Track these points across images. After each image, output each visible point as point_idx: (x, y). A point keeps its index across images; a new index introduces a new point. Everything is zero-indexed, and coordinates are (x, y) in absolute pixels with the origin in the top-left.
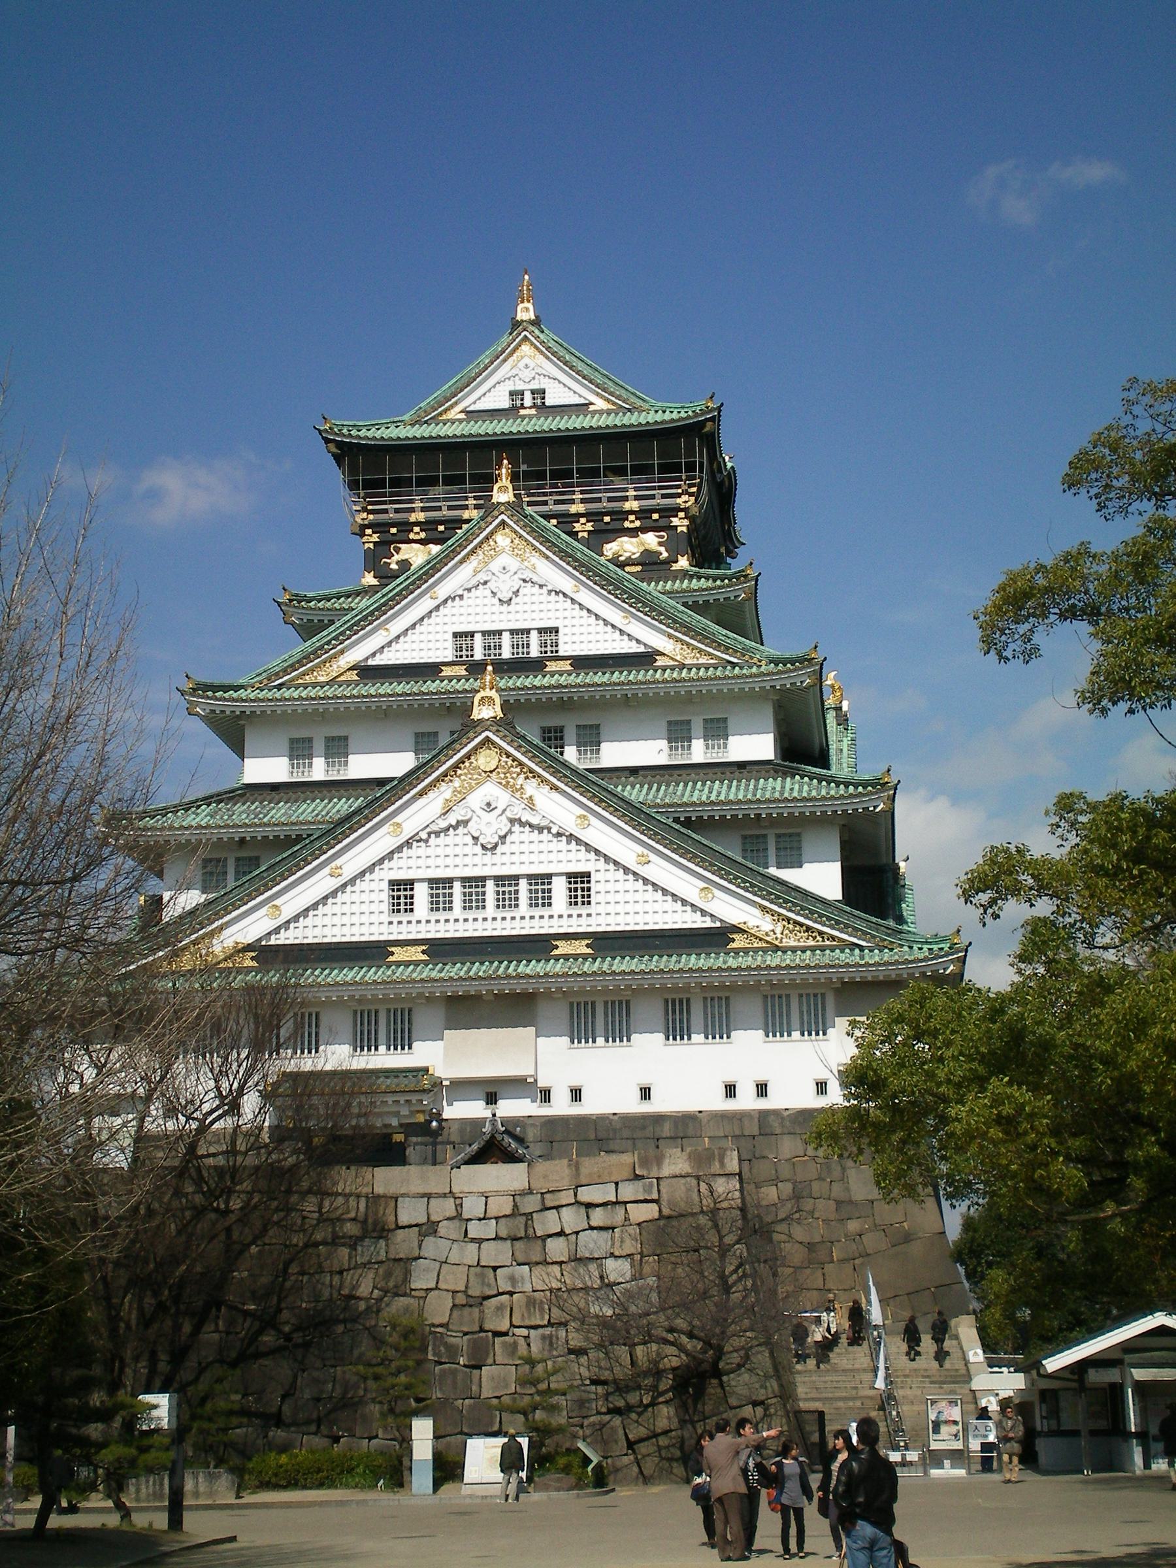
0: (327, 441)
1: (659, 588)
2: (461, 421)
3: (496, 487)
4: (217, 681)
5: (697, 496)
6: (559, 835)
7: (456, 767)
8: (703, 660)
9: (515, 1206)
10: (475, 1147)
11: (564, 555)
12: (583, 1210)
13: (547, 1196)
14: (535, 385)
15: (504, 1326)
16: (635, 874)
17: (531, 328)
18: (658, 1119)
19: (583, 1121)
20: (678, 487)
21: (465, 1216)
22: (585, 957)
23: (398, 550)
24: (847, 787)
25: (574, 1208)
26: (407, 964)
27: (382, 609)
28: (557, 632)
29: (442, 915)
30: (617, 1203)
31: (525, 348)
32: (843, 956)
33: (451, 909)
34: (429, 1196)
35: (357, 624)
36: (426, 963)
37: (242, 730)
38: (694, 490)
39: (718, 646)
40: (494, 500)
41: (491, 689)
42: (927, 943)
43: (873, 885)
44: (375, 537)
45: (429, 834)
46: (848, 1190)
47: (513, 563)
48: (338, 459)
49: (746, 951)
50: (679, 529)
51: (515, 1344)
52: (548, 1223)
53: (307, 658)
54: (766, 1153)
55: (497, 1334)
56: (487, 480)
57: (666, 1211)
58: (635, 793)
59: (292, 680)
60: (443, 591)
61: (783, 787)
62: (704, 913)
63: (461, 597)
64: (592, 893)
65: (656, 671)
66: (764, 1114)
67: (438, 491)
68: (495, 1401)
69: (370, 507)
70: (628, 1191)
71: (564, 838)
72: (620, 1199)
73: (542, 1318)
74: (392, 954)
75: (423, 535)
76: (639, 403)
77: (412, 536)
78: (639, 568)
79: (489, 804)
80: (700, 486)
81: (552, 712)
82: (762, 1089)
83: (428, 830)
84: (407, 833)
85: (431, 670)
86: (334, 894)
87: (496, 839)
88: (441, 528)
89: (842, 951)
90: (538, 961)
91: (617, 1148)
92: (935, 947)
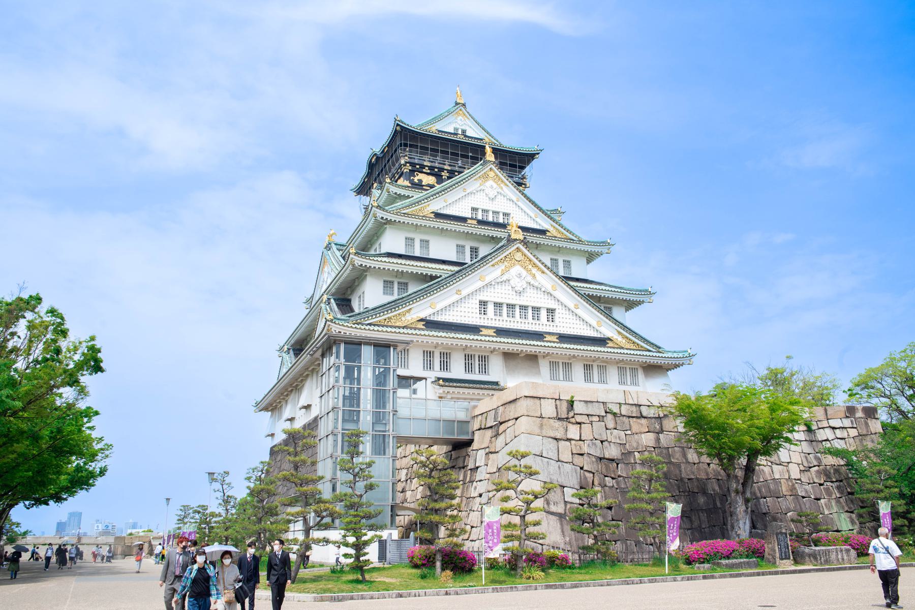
0: (398, 125)
14: (464, 128)
47: (495, 185)
84: (488, 279)
85: (463, 220)
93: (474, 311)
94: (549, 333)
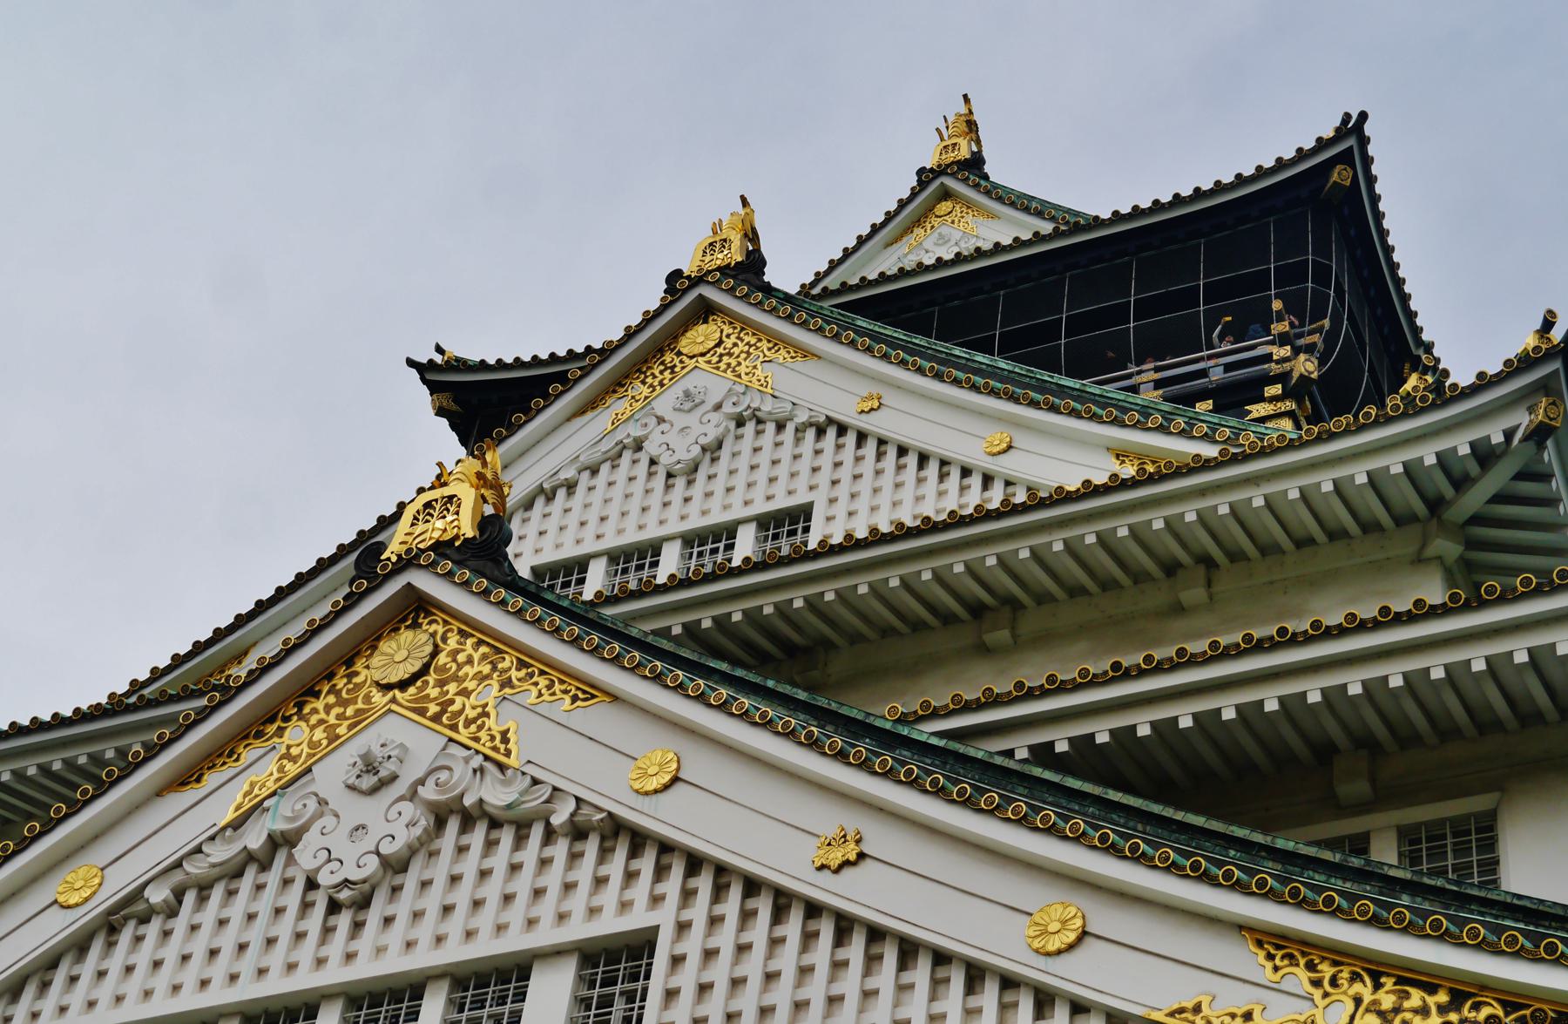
16: (813, 910)
28: (808, 519)
31: (945, 207)
45: (179, 894)
79: (370, 766)
83: (177, 877)
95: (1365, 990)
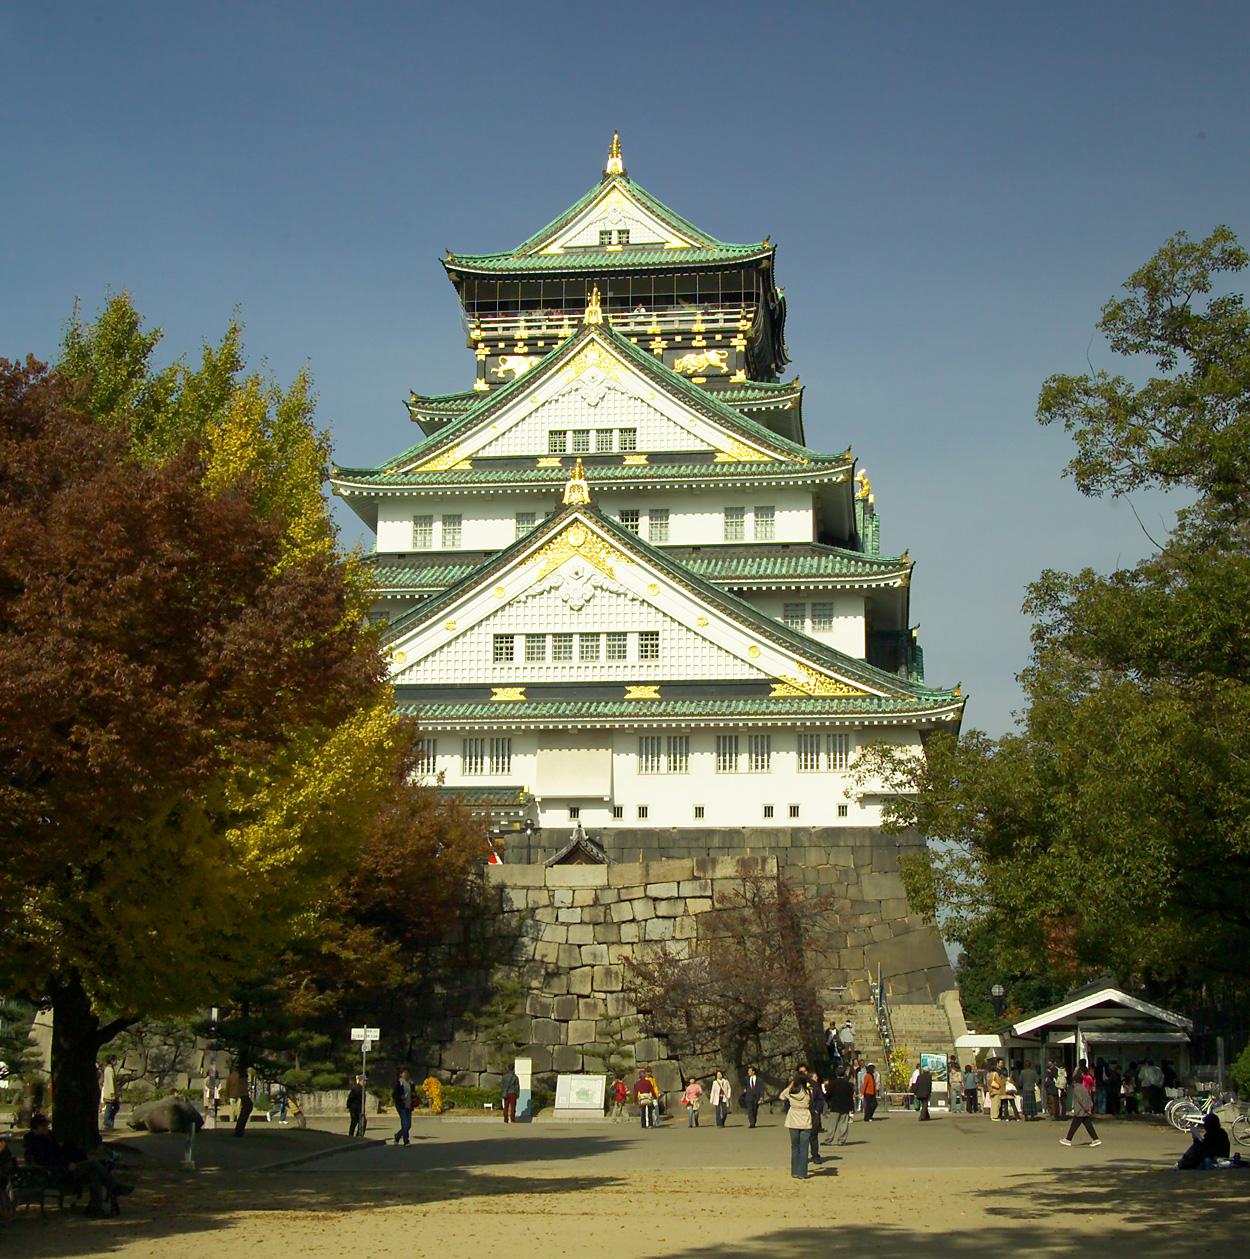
0: (449, 271)
1: (720, 396)
2: (559, 255)
3: (587, 310)
4: (356, 467)
5: (753, 321)
6: (633, 600)
7: (550, 541)
8: (756, 457)
9: (597, 898)
10: (564, 851)
11: (642, 368)
12: (651, 903)
13: (622, 891)
14: (623, 228)
15: (587, 990)
17: (619, 179)
18: (710, 833)
19: (648, 833)
20: (739, 313)
21: (556, 905)
22: (653, 701)
23: (504, 361)
24: (871, 566)
25: (645, 900)
26: (507, 703)
27: (490, 411)
29: (536, 664)
30: (679, 898)
32: (864, 705)
33: (543, 659)
34: (528, 888)
35: (470, 422)
36: (523, 703)
37: (377, 506)
38: (751, 316)
39: (769, 447)
40: (585, 322)
41: (580, 477)
42: (933, 695)
43: (892, 645)
44: (487, 351)
46: (861, 891)
48: (457, 285)
49: (785, 699)
50: (738, 349)
51: (595, 1006)
52: (623, 912)
53: (429, 449)
54: (795, 861)
55: (580, 996)
56: (580, 305)
57: (717, 906)
58: (697, 567)
59: (417, 468)
60: (541, 395)
61: (819, 565)
62: (751, 666)
63: (557, 401)
64: (660, 648)
65: (716, 466)
66: (796, 831)
67: (538, 314)
68: (580, 1048)
69: (483, 326)
70: (687, 889)
71: (638, 603)
72: (681, 895)
73: (617, 985)
74: (496, 694)
75: (526, 349)
76: (707, 242)
77: (516, 350)
78: (704, 380)
79: (577, 574)
80: (756, 313)
81: (628, 496)
82: (794, 811)
83: (526, 594)
85: (531, 461)
86: (449, 644)
87: (582, 602)
88: (541, 344)
89: (864, 701)
90: (614, 703)
91: (676, 855)
92: (940, 699)
93: (481, 656)
94: (638, 684)
95: (818, 676)
